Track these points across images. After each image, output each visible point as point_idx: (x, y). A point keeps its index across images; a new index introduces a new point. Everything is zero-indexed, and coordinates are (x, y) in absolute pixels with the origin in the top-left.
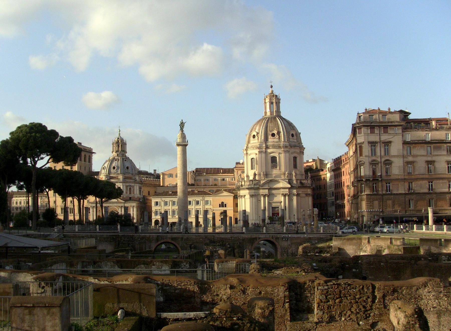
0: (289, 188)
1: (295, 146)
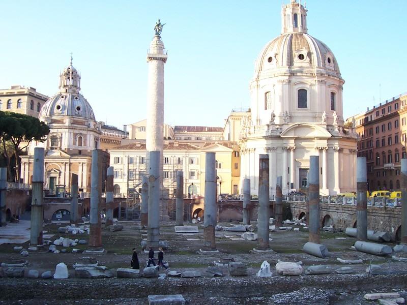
0: (328, 139)
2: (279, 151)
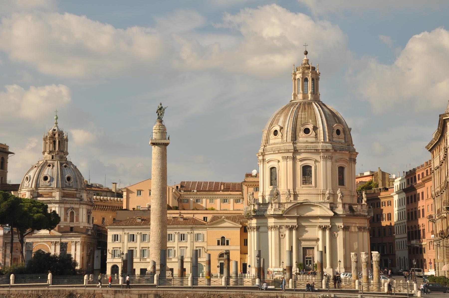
0: (331, 218)
1: (342, 150)
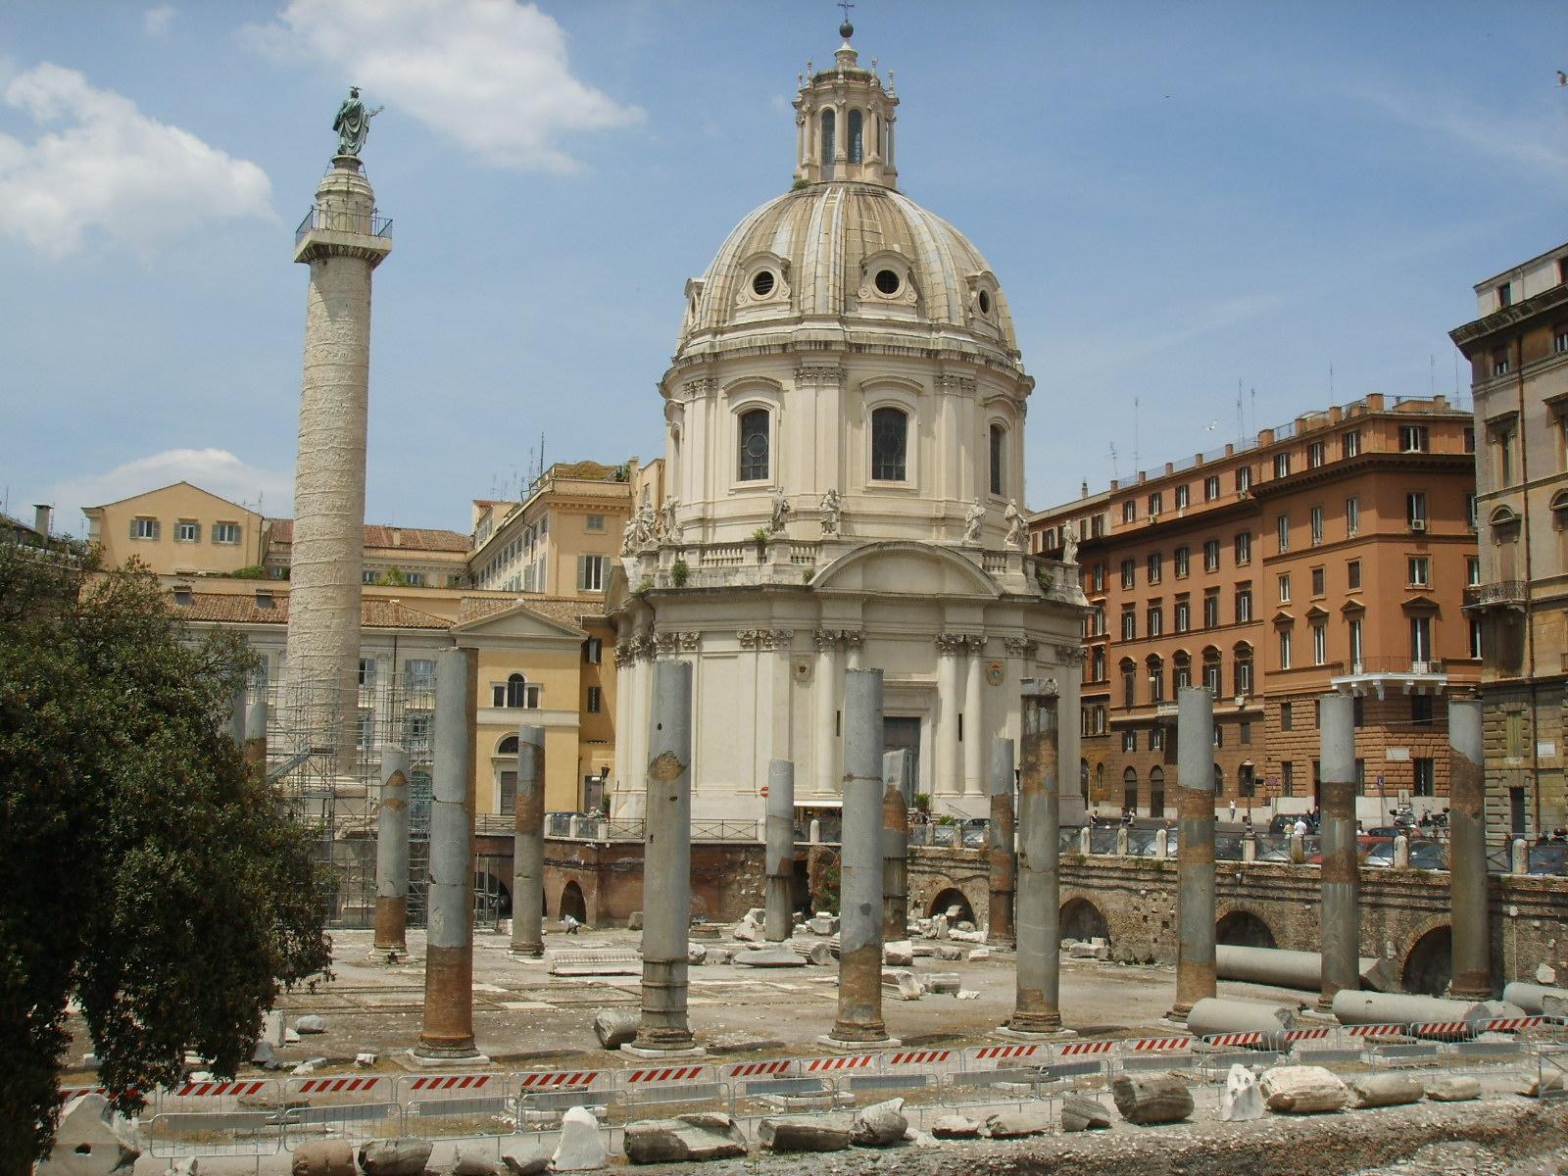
0: (989, 606)
2: (802, 644)
